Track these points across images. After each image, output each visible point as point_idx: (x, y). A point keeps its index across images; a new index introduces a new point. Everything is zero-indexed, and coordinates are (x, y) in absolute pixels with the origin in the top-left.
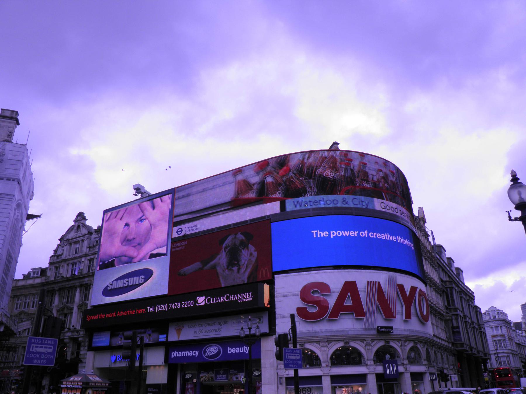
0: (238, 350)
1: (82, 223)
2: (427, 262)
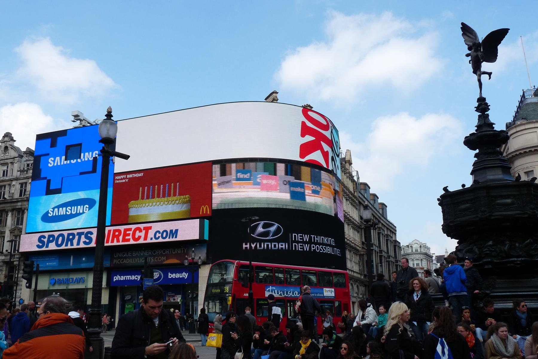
0: (178, 276)
1: (11, 145)
2: (348, 202)
